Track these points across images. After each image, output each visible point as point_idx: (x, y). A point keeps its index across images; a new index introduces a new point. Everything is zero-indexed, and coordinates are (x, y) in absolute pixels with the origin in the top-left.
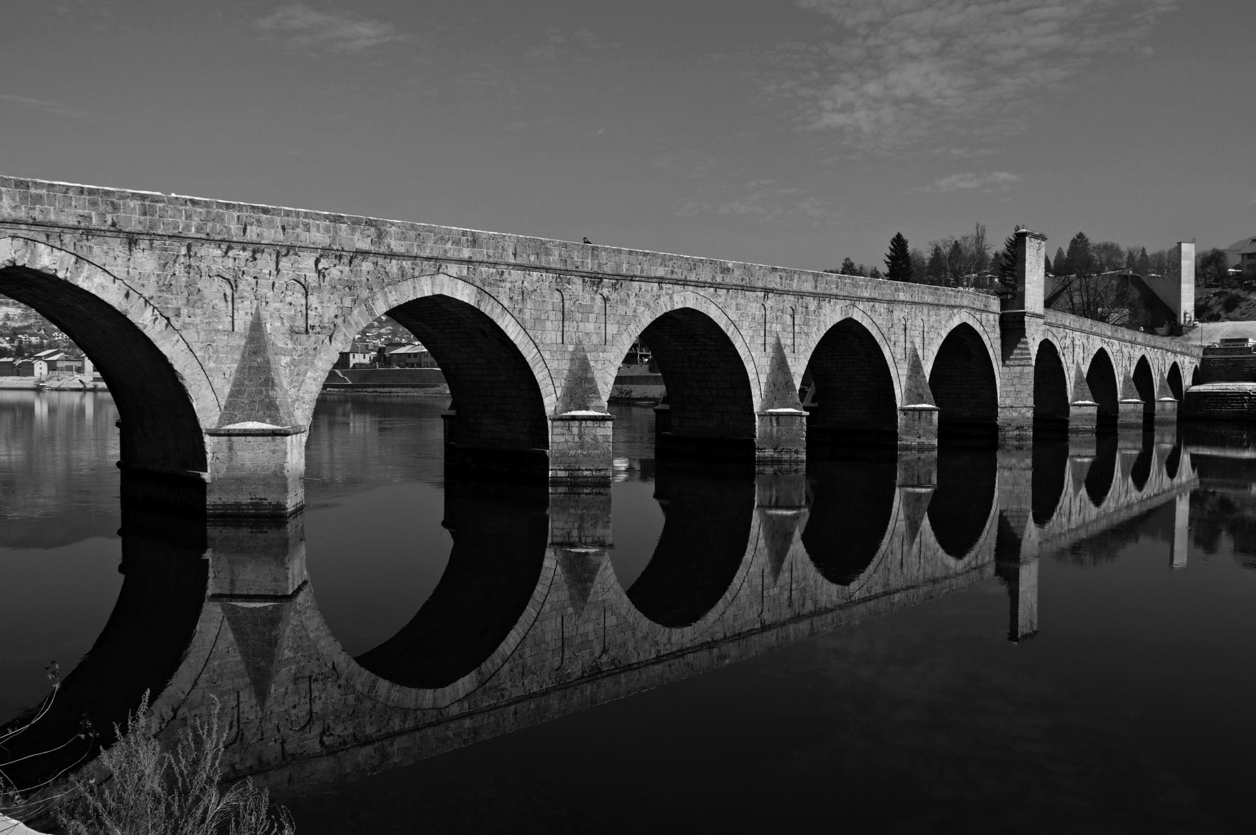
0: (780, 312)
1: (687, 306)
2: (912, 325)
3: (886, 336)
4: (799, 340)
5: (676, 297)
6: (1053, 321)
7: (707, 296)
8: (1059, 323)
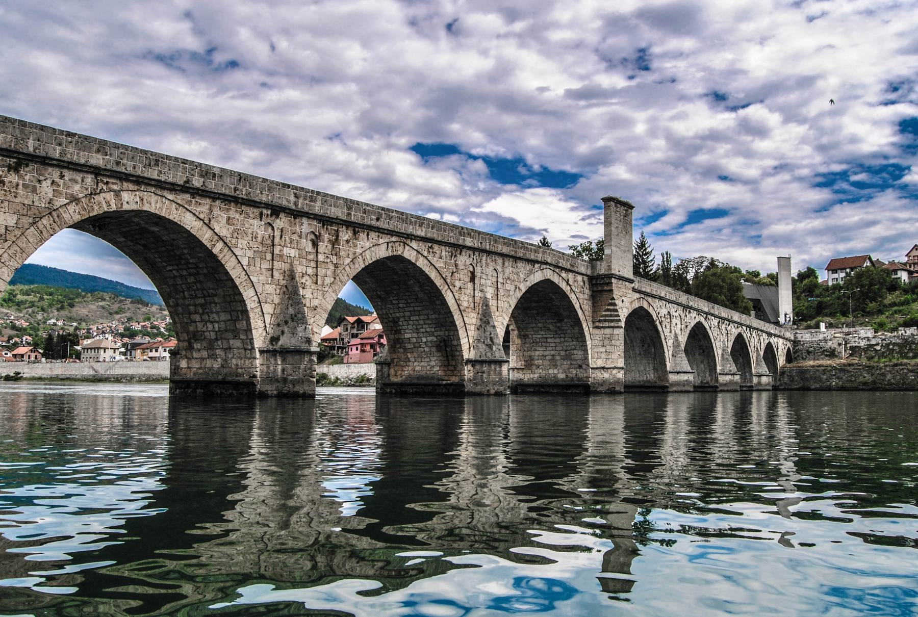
0: (296, 235)
1: (146, 208)
2: (482, 273)
3: (448, 281)
4: (324, 270)
5: (125, 196)
6: (648, 290)
7: (179, 202)
8: (655, 293)
